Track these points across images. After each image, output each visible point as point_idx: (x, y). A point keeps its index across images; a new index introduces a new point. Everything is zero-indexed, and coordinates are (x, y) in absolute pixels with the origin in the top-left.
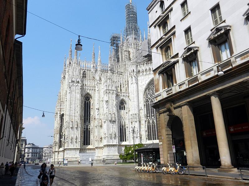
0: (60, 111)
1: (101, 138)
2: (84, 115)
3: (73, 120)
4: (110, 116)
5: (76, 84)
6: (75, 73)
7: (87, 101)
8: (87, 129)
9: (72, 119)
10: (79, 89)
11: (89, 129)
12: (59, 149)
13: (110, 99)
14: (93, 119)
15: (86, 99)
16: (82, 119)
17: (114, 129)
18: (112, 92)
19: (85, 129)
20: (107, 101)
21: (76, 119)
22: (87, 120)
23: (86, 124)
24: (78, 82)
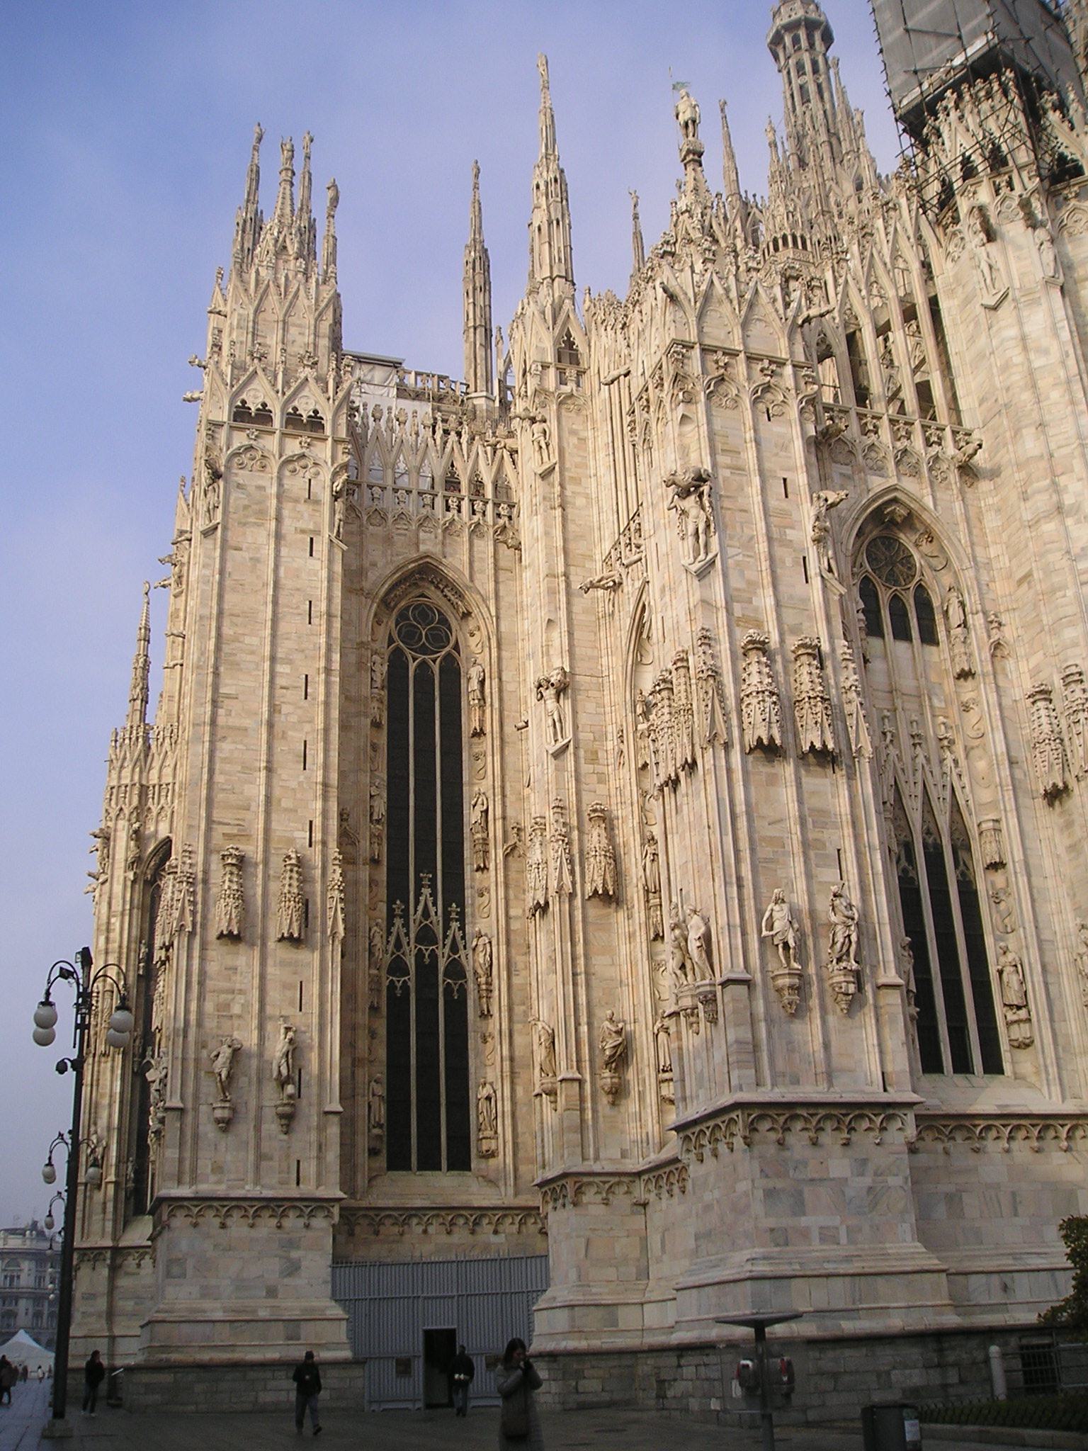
0: (141, 811)
1: (621, 1058)
2: (381, 807)
3: (254, 850)
4: (756, 677)
5: (293, 447)
6: (273, 340)
7: (423, 650)
8: (427, 970)
9: (245, 836)
10: (326, 497)
11: (456, 970)
12: (126, 1223)
13: (738, 469)
14: (497, 854)
15: (409, 635)
16: (364, 847)
17: (831, 874)
18: (761, 380)
19: (398, 967)
20: (694, 486)
21: (291, 841)
22: (426, 863)
23: (415, 917)
24: (315, 423)
